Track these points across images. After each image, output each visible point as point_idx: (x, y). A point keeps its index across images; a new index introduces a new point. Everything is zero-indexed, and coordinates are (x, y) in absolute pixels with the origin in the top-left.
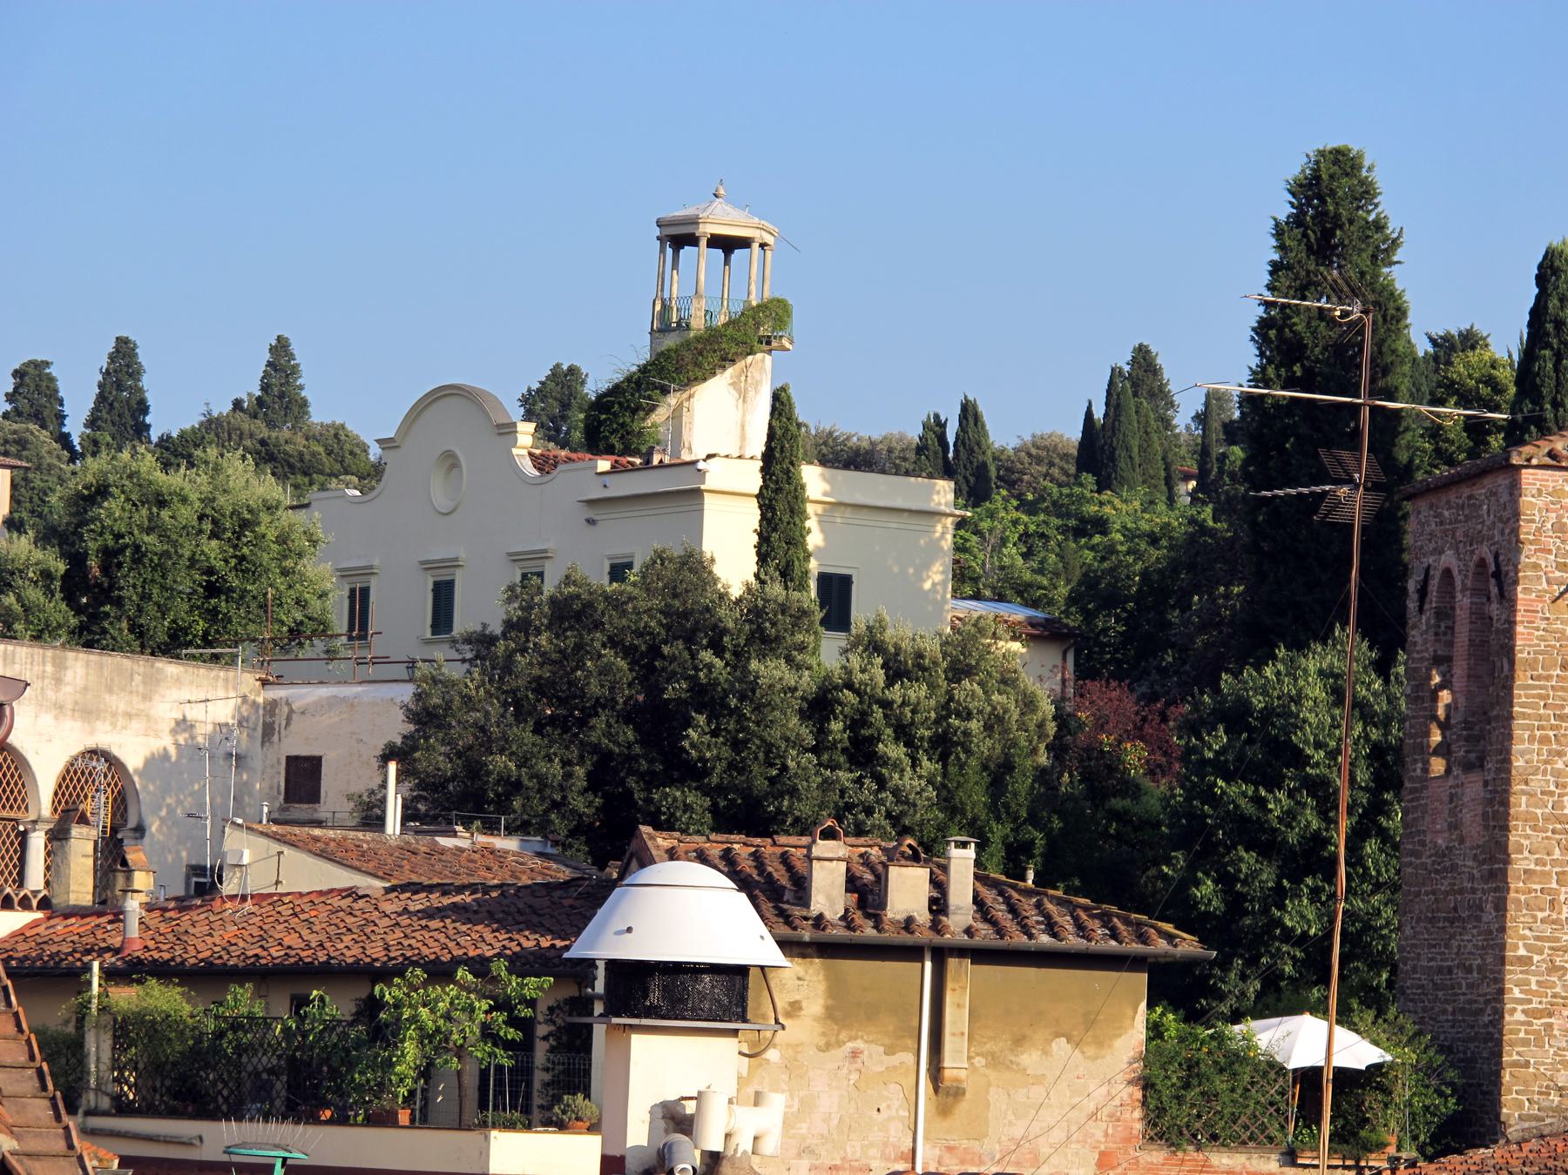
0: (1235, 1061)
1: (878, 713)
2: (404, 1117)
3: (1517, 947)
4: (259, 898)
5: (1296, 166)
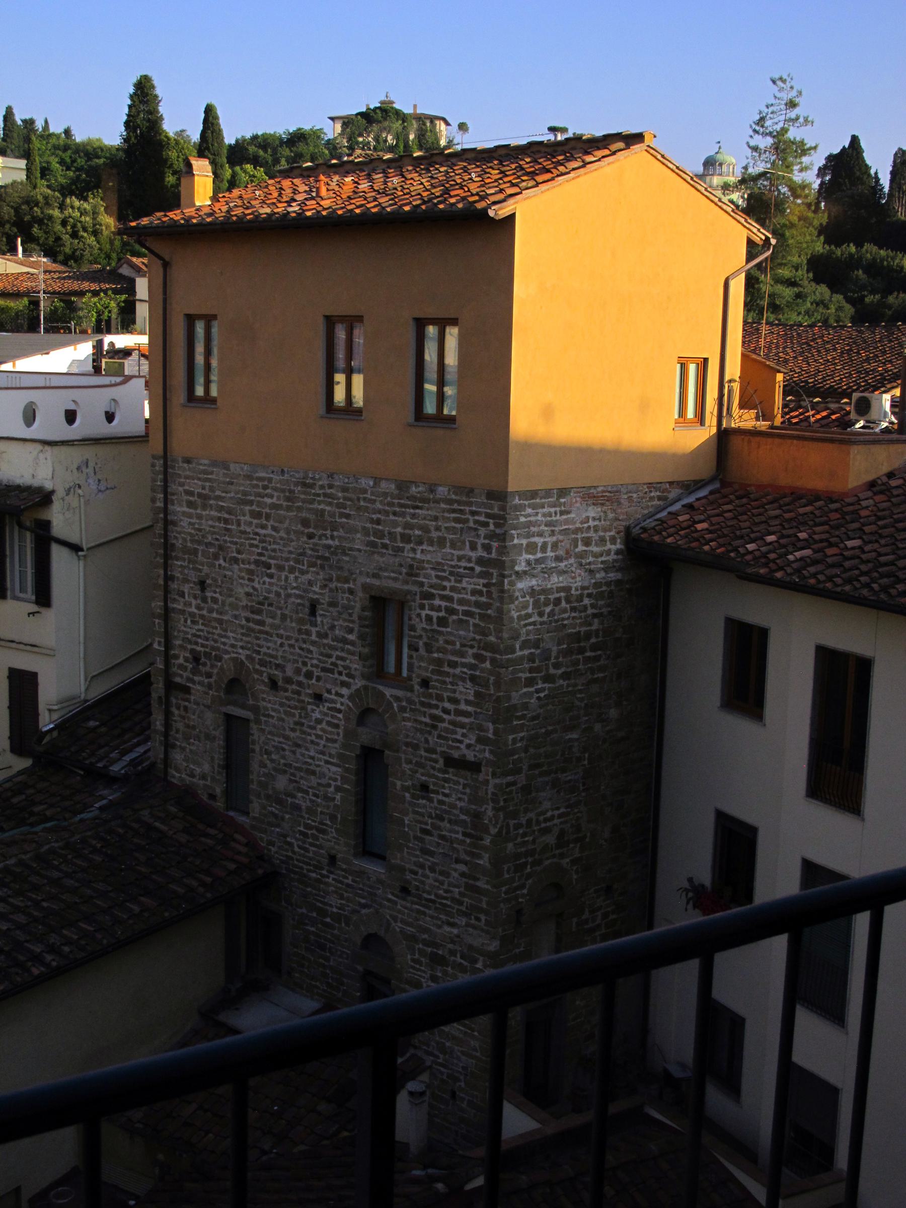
1: (79, 225)
2: (89, 331)
5: (135, 80)
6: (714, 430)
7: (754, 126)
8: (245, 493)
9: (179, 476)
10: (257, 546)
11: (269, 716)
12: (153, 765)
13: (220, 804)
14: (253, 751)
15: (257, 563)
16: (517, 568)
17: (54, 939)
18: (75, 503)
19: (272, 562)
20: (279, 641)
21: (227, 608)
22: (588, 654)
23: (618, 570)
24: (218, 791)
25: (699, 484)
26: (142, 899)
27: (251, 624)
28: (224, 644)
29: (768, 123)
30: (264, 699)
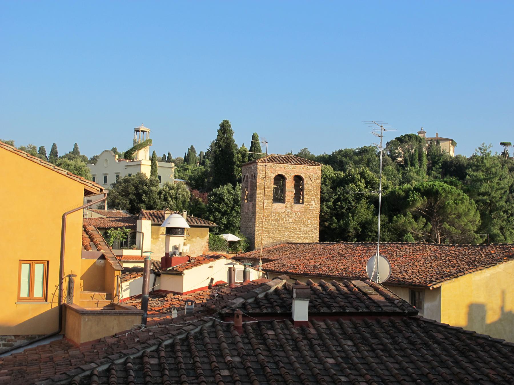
0: (220, 240)
3: (257, 225)
4: (89, 219)
5: (220, 122)
6: (56, 305)
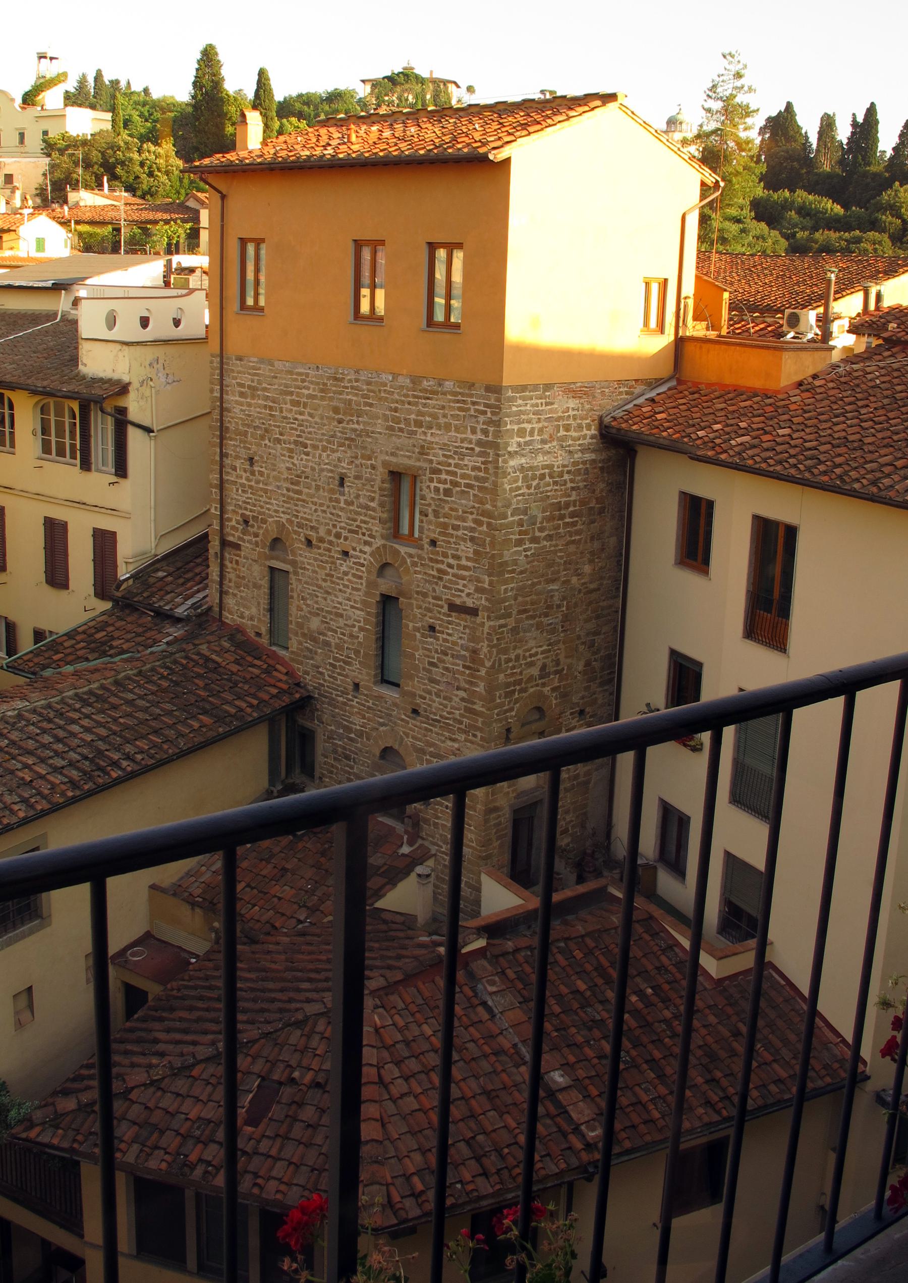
5: (201, 48)
7: (708, 92)
8: (286, 386)
9: (233, 371)
10: (296, 430)
11: (304, 569)
12: (210, 609)
13: (264, 641)
14: (292, 597)
15: (296, 443)
16: (509, 449)
17: (128, 748)
18: (147, 393)
19: (308, 442)
20: (314, 508)
21: (271, 480)
22: (567, 520)
23: (594, 451)
24: (264, 630)
25: (659, 382)
26: (201, 716)
27: (291, 494)
28: (269, 509)
29: (719, 90)
30: (301, 555)
